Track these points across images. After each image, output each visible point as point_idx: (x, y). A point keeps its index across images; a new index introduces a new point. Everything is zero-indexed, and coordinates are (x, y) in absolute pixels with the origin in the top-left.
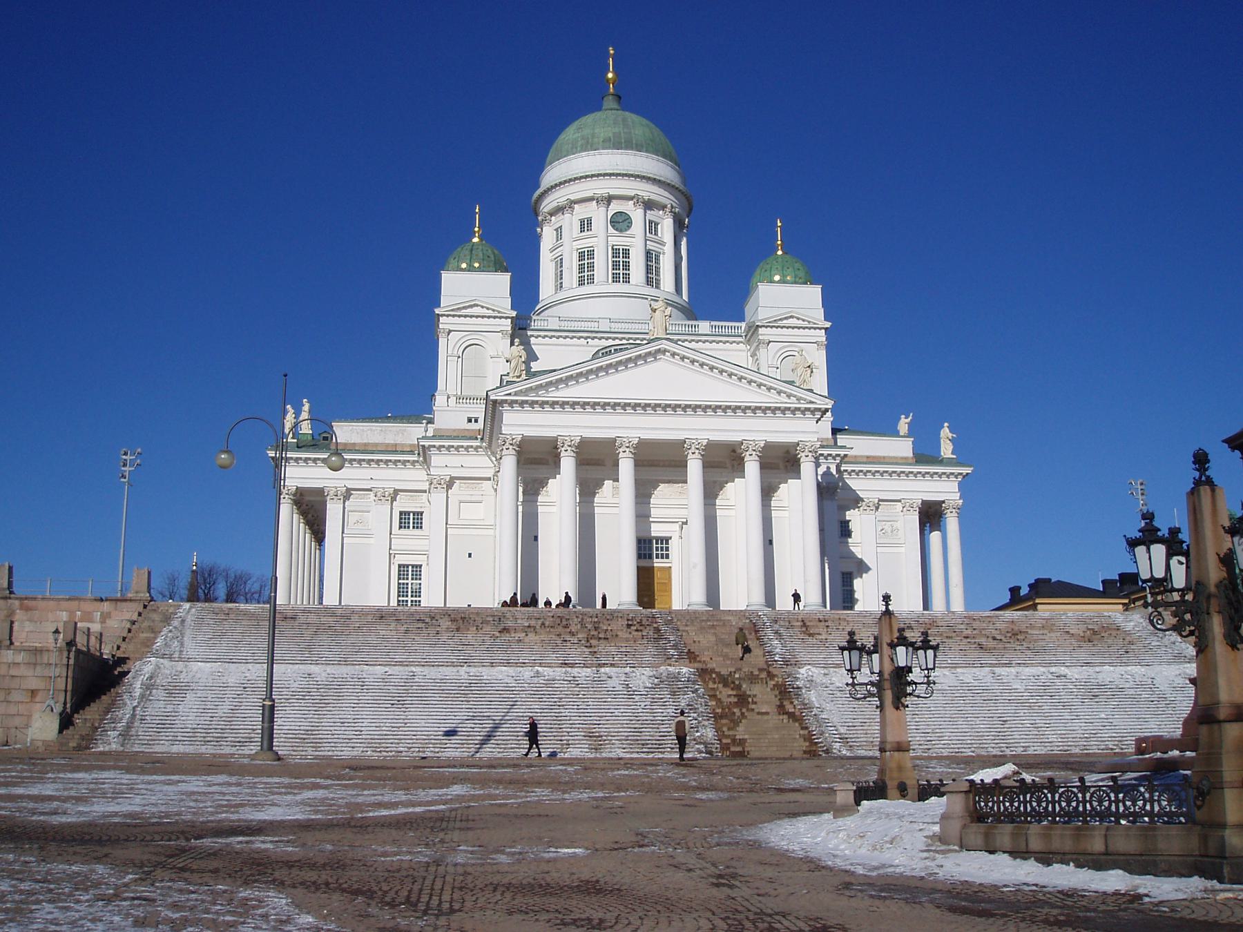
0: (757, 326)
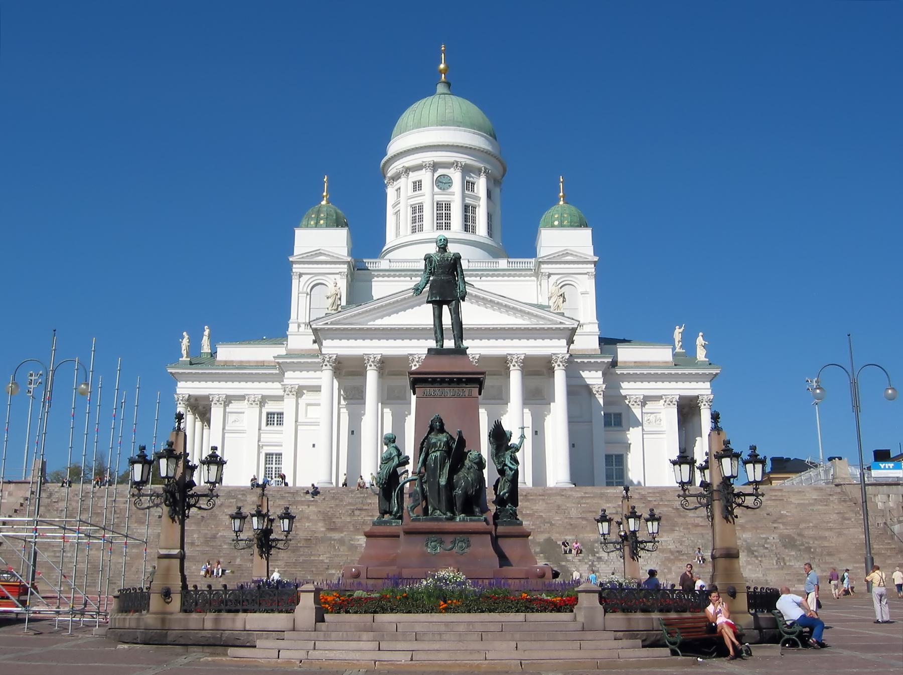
0: (540, 262)
